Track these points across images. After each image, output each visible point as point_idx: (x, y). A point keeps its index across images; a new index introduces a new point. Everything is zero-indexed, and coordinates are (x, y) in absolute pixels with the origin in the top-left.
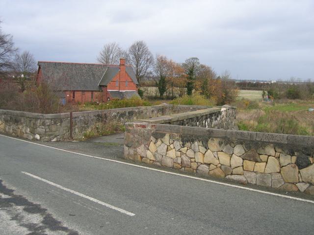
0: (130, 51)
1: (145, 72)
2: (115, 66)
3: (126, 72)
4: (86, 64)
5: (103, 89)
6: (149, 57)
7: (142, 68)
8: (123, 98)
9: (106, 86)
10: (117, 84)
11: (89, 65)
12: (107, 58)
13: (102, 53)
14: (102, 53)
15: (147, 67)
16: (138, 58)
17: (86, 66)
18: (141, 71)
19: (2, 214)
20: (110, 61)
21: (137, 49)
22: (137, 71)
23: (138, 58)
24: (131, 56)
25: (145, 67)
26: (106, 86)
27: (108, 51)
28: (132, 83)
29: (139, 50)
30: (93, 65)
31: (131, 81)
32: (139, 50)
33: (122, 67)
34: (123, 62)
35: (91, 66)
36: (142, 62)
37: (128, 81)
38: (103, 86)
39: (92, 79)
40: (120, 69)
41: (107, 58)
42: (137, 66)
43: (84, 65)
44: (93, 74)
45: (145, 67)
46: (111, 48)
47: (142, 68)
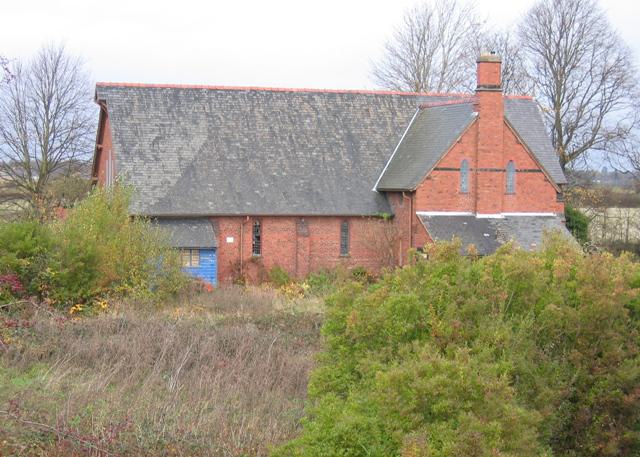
0: (524, 34)
1: (595, 131)
2: (457, 97)
3: (506, 123)
4: (320, 93)
5: (398, 207)
6: (612, 61)
7: (581, 109)
8: (490, 246)
9: (411, 193)
10: (465, 183)
11: (332, 95)
12: (420, 70)
13: (398, 46)
14: (398, 46)
15: (603, 108)
16: (560, 65)
17: (319, 103)
18: (571, 129)
19: (635, 235)
20: (433, 81)
21: (557, 20)
22: (557, 126)
23: (560, 65)
24: (530, 61)
25: (592, 108)
26: (411, 193)
27: (422, 39)
28: (538, 178)
29: (564, 28)
30: (351, 96)
31: (533, 166)
32: (564, 28)
33: (487, 98)
34: (493, 73)
35: (340, 102)
36: (580, 83)
37: (516, 165)
38: (398, 193)
39: (346, 159)
40: (477, 106)
41: (420, 70)
42: (557, 105)
43: (310, 96)
44: (350, 137)
45: (592, 108)
46: (435, 22)
47: (581, 109)
